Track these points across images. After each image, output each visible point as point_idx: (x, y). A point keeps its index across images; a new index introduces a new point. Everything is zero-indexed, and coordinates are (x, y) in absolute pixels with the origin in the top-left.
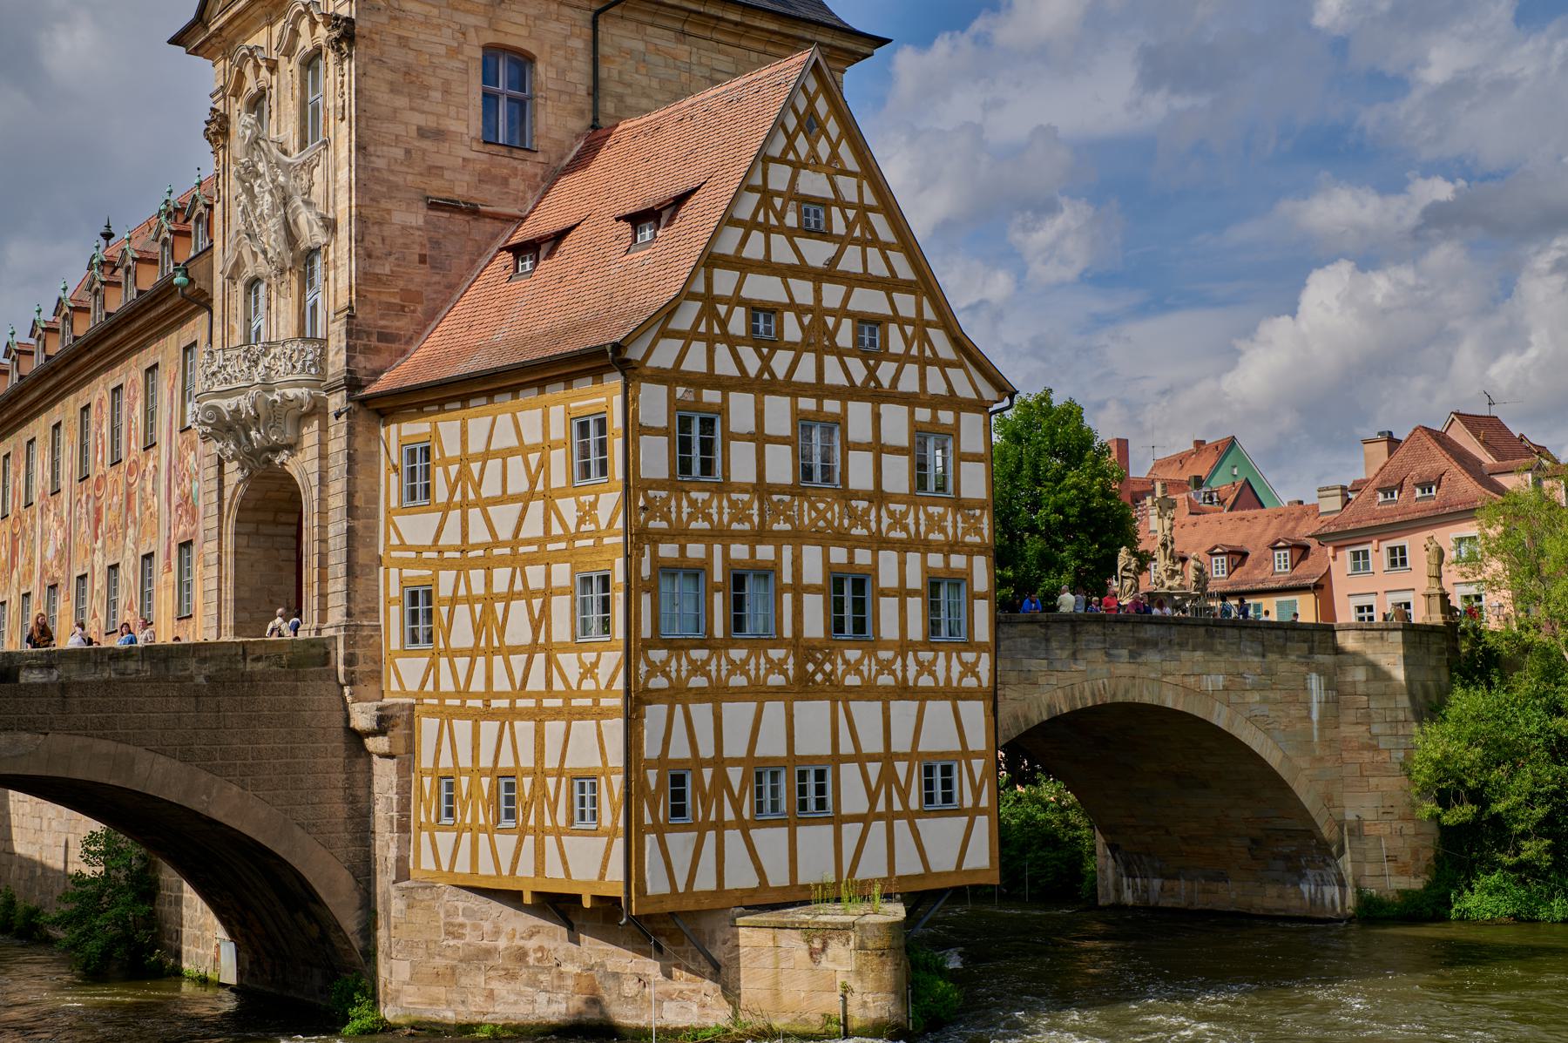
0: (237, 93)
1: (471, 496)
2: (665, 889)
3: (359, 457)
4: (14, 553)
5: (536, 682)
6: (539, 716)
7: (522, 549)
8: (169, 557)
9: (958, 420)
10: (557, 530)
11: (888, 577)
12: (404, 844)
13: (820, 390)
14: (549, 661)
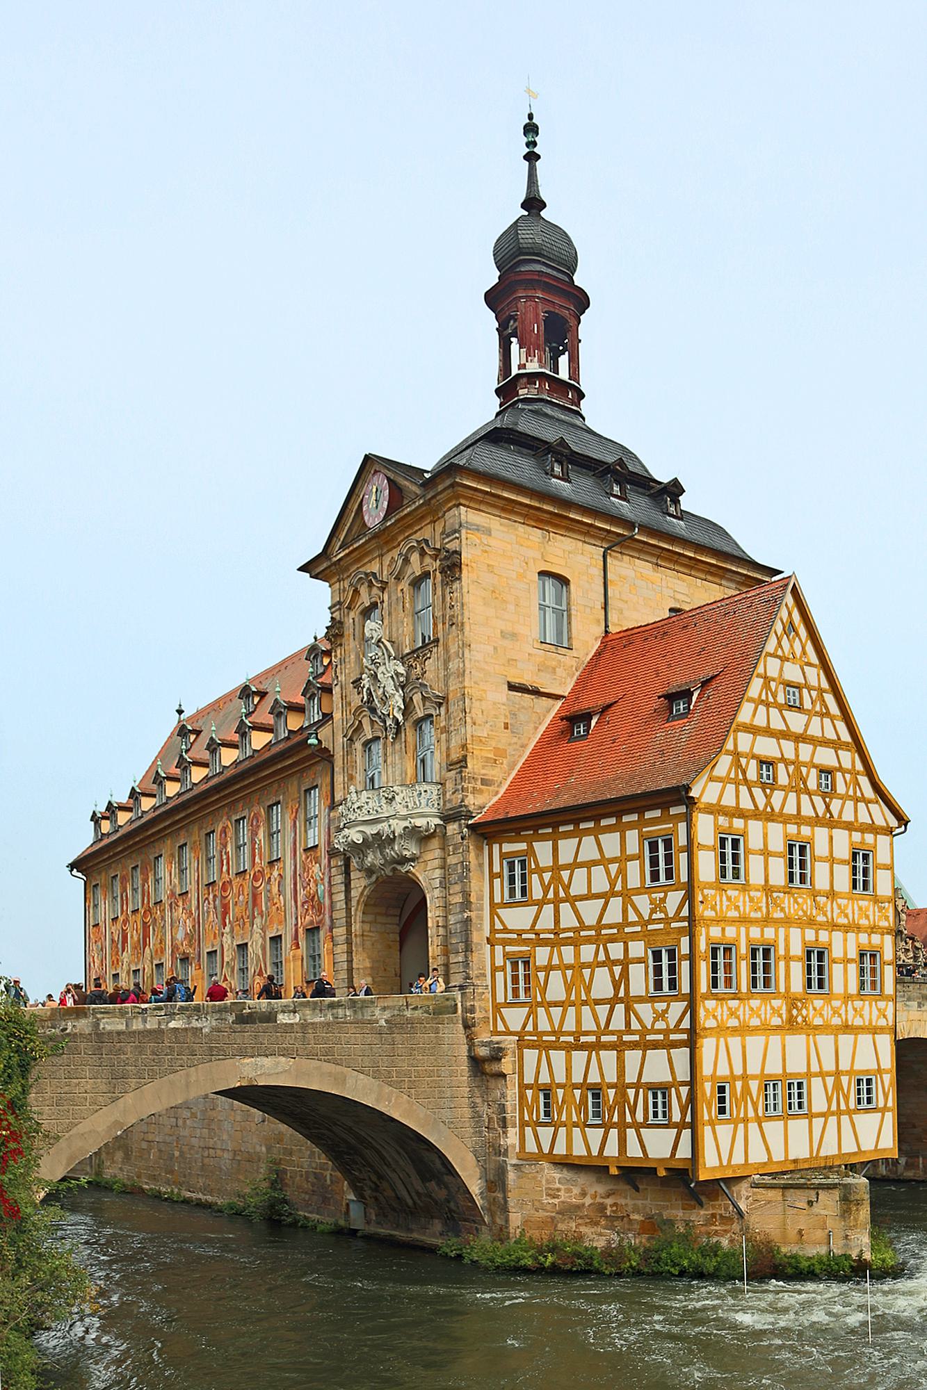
1: (562, 894)
3: (472, 867)
4: (146, 935)
5: (618, 1023)
6: (620, 1047)
7: (603, 932)
10: (632, 917)
14: (628, 1010)
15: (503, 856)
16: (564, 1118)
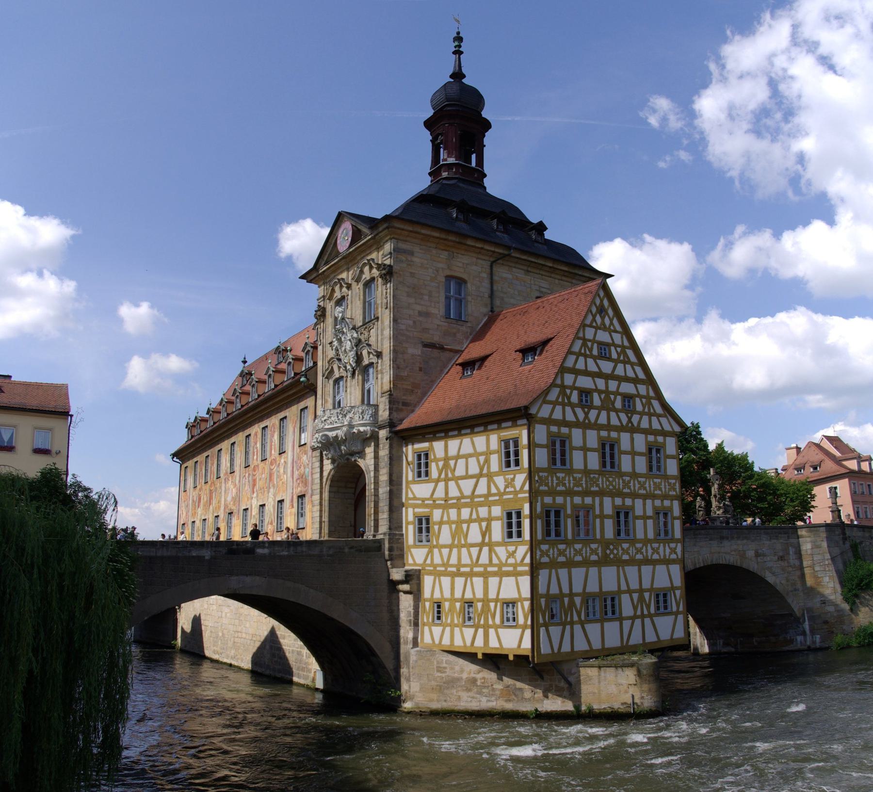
0: (330, 299)
1: (450, 475)
2: (549, 651)
4: (211, 498)
5: (484, 559)
7: (476, 500)
9: (665, 440)
10: (494, 490)
11: (639, 511)
12: (416, 632)
13: (608, 427)
14: (490, 551)
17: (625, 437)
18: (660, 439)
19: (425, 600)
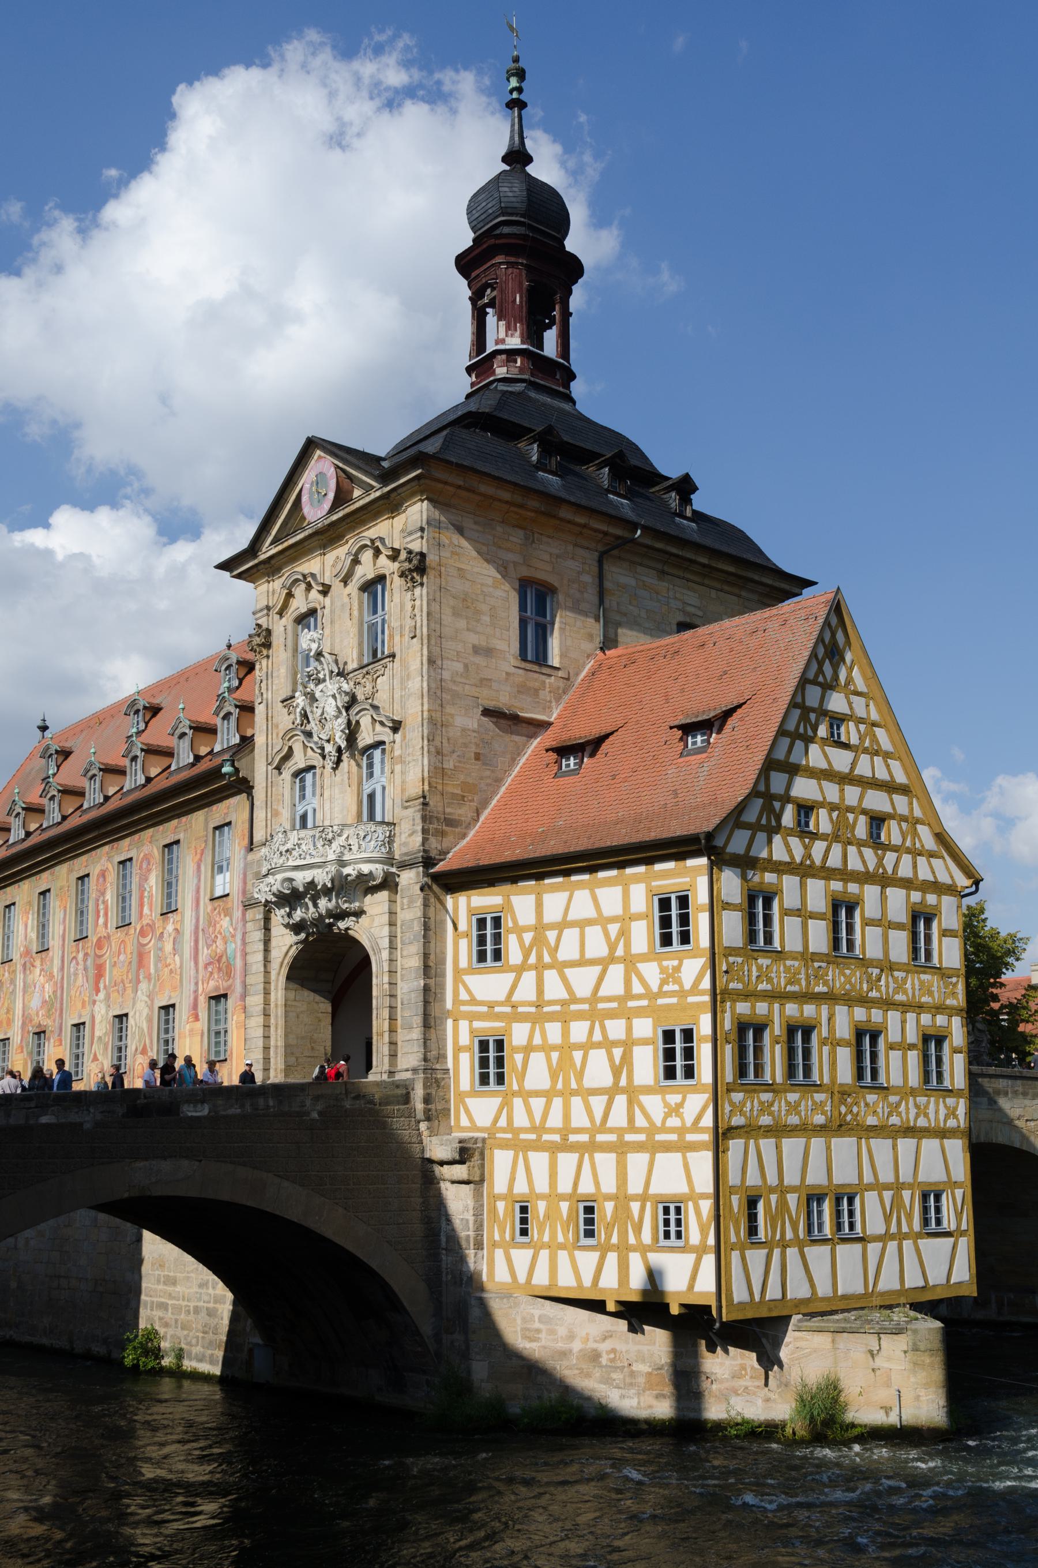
1: (547, 959)
5: (618, 1117)
6: (621, 1149)
7: (600, 1006)
8: (195, 1006)
10: (637, 988)
11: (893, 1034)
13: (844, 874)
15: (471, 912)
16: (546, 1238)
17: (871, 893)
18: (931, 899)
19: (496, 1198)
